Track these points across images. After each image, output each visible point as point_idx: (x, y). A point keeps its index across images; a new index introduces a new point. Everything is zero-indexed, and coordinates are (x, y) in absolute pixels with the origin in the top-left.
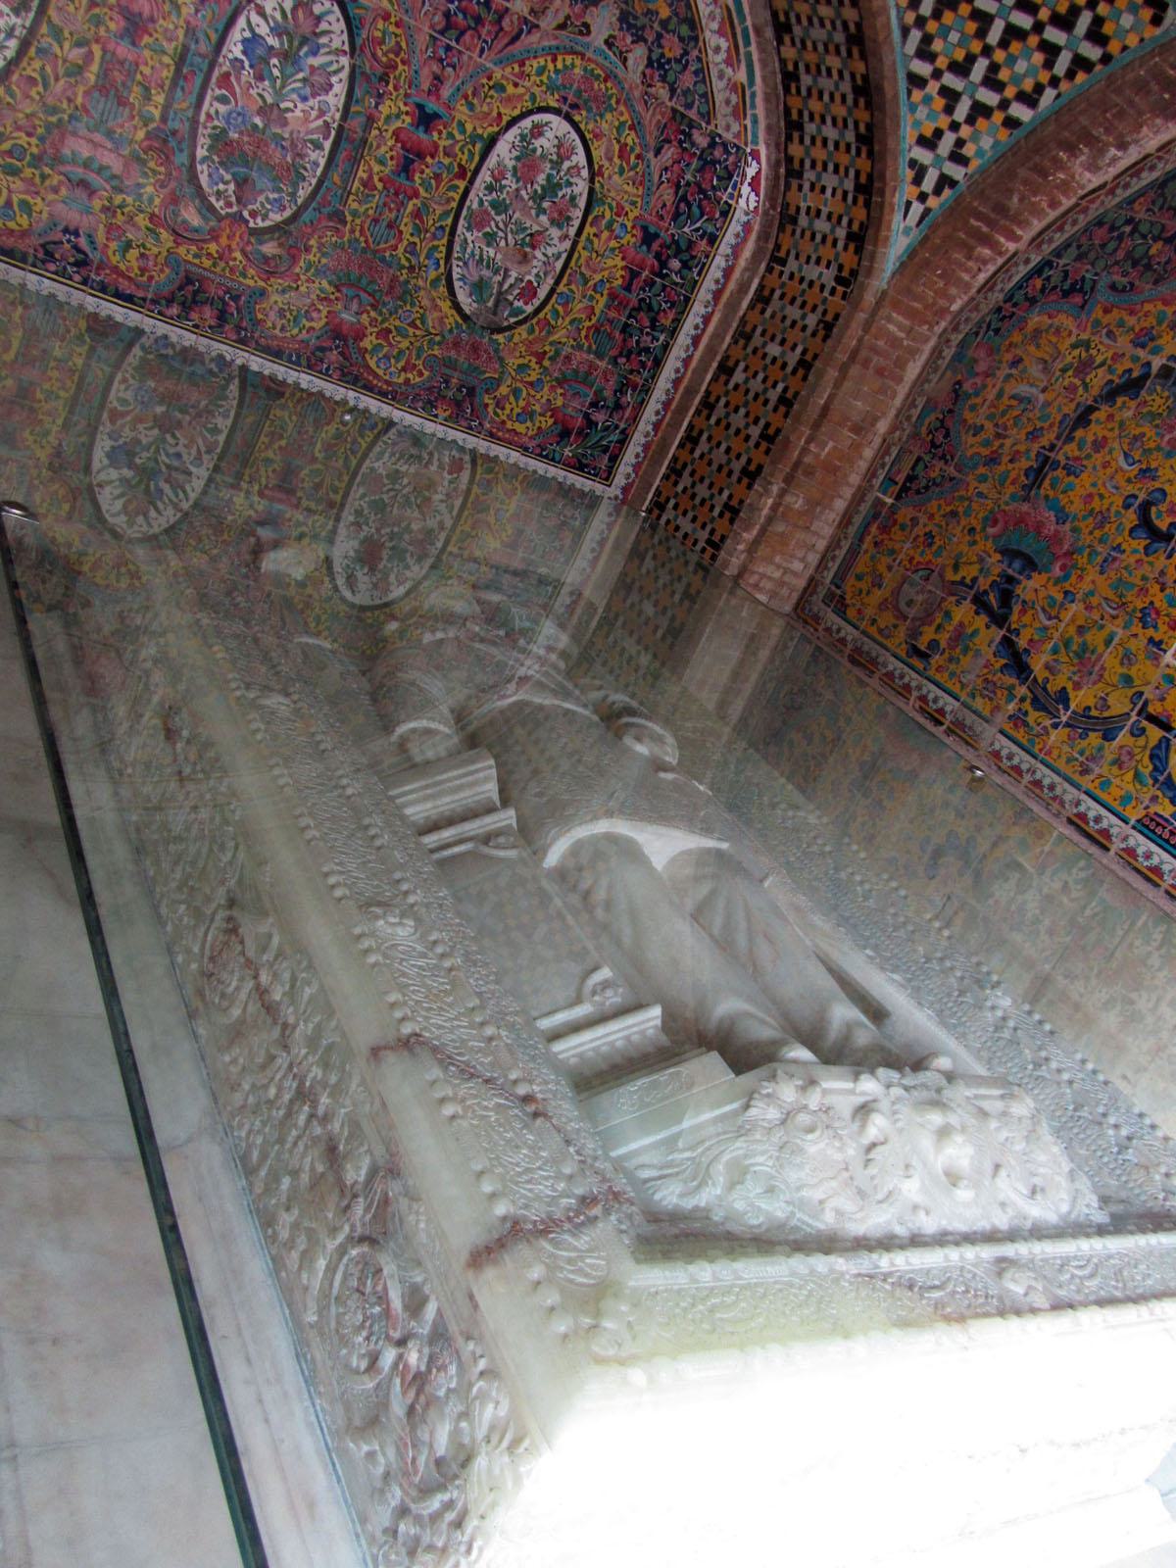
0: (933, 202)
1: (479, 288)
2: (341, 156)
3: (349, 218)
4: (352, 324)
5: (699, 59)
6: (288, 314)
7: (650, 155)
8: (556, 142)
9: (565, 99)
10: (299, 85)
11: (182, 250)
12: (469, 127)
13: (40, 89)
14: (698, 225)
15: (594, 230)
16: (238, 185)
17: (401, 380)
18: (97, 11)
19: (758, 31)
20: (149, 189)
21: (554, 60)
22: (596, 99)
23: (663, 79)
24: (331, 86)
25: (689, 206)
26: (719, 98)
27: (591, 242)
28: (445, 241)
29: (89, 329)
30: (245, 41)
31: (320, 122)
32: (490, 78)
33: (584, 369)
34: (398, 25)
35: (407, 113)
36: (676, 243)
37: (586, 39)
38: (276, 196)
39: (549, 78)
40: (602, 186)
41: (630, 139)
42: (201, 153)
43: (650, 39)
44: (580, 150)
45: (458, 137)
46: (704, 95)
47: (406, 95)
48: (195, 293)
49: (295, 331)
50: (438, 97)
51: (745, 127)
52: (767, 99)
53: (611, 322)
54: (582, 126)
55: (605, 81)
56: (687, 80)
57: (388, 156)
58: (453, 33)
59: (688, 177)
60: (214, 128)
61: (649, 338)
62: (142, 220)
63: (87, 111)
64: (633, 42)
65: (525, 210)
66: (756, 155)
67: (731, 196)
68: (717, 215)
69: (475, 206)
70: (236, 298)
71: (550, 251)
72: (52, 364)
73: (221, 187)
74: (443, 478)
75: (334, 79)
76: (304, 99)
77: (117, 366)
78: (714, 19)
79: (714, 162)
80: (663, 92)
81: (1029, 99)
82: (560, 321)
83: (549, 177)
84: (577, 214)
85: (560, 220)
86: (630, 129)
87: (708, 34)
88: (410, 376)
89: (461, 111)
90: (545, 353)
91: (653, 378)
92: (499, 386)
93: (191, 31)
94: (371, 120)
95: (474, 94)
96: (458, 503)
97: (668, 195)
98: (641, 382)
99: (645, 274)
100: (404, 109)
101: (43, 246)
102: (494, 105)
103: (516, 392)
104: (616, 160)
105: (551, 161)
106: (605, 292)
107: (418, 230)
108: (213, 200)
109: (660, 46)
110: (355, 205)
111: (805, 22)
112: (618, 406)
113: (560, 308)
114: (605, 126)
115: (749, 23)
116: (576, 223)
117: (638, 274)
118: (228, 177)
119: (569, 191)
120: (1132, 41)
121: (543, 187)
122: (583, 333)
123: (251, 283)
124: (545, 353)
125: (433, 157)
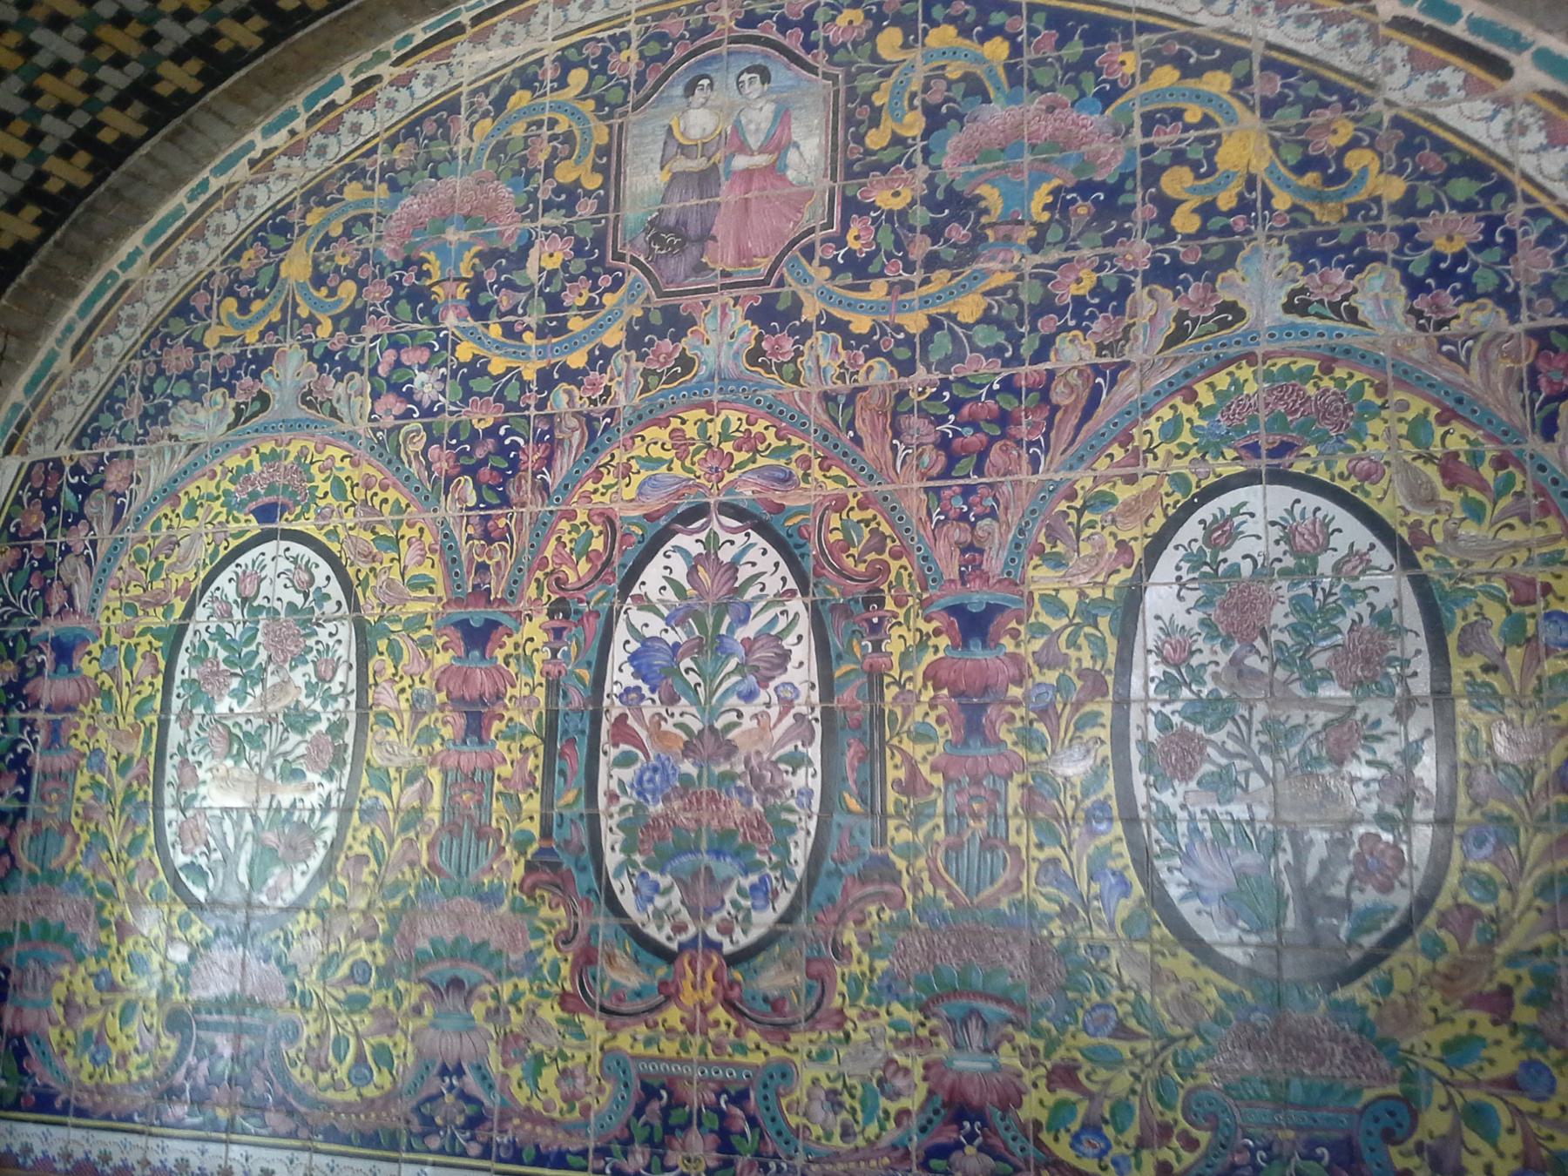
2: (850, 756)
3: (901, 864)
4: (984, 1074)
5: (1537, 213)
6: (846, 1098)
7: (1534, 443)
8: (1276, 532)
9: (1254, 449)
10: (735, 679)
11: (623, 1041)
12: (1070, 598)
13: (373, 865)
16: (686, 888)
18: (425, 721)
20: (550, 953)
21: (1191, 397)
22: (1325, 413)
23: (1469, 293)
24: (786, 656)
28: (1118, 829)
30: (633, 658)
31: (789, 720)
32: (1072, 496)
34: (862, 506)
35: (937, 632)
37: (1241, 327)
38: (754, 878)
39: (1194, 431)
40: (1442, 562)
42: (612, 859)
43: (1389, 249)
45: (1055, 624)
47: (924, 604)
48: (666, 1112)
54: (1322, 475)
55: (1327, 370)
57: (931, 720)
58: (967, 464)
60: (624, 809)
62: (550, 1013)
64: (1350, 275)
69: (1154, 734)
70: (740, 1098)
73: (660, 902)
75: (791, 639)
76: (749, 696)
78: (1524, 130)
80: (1482, 317)
83: (1298, 604)
86: (1443, 420)
87: (1527, 163)
89: (1041, 578)
92: (1414, 1116)
93: (554, 687)
94: (875, 678)
95: (1052, 538)
100: (928, 628)
101: (417, 1110)
102: (1101, 537)
103: (1478, 1117)
104: (1445, 495)
105: (1285, 573)
107: (1048, 834)
108: (651, 930)
110: (905, 835)
118: (665, 881)
121: (1294, 629)
123: (757, 1059)
124: (1506, 991)
125: (1019, 682)
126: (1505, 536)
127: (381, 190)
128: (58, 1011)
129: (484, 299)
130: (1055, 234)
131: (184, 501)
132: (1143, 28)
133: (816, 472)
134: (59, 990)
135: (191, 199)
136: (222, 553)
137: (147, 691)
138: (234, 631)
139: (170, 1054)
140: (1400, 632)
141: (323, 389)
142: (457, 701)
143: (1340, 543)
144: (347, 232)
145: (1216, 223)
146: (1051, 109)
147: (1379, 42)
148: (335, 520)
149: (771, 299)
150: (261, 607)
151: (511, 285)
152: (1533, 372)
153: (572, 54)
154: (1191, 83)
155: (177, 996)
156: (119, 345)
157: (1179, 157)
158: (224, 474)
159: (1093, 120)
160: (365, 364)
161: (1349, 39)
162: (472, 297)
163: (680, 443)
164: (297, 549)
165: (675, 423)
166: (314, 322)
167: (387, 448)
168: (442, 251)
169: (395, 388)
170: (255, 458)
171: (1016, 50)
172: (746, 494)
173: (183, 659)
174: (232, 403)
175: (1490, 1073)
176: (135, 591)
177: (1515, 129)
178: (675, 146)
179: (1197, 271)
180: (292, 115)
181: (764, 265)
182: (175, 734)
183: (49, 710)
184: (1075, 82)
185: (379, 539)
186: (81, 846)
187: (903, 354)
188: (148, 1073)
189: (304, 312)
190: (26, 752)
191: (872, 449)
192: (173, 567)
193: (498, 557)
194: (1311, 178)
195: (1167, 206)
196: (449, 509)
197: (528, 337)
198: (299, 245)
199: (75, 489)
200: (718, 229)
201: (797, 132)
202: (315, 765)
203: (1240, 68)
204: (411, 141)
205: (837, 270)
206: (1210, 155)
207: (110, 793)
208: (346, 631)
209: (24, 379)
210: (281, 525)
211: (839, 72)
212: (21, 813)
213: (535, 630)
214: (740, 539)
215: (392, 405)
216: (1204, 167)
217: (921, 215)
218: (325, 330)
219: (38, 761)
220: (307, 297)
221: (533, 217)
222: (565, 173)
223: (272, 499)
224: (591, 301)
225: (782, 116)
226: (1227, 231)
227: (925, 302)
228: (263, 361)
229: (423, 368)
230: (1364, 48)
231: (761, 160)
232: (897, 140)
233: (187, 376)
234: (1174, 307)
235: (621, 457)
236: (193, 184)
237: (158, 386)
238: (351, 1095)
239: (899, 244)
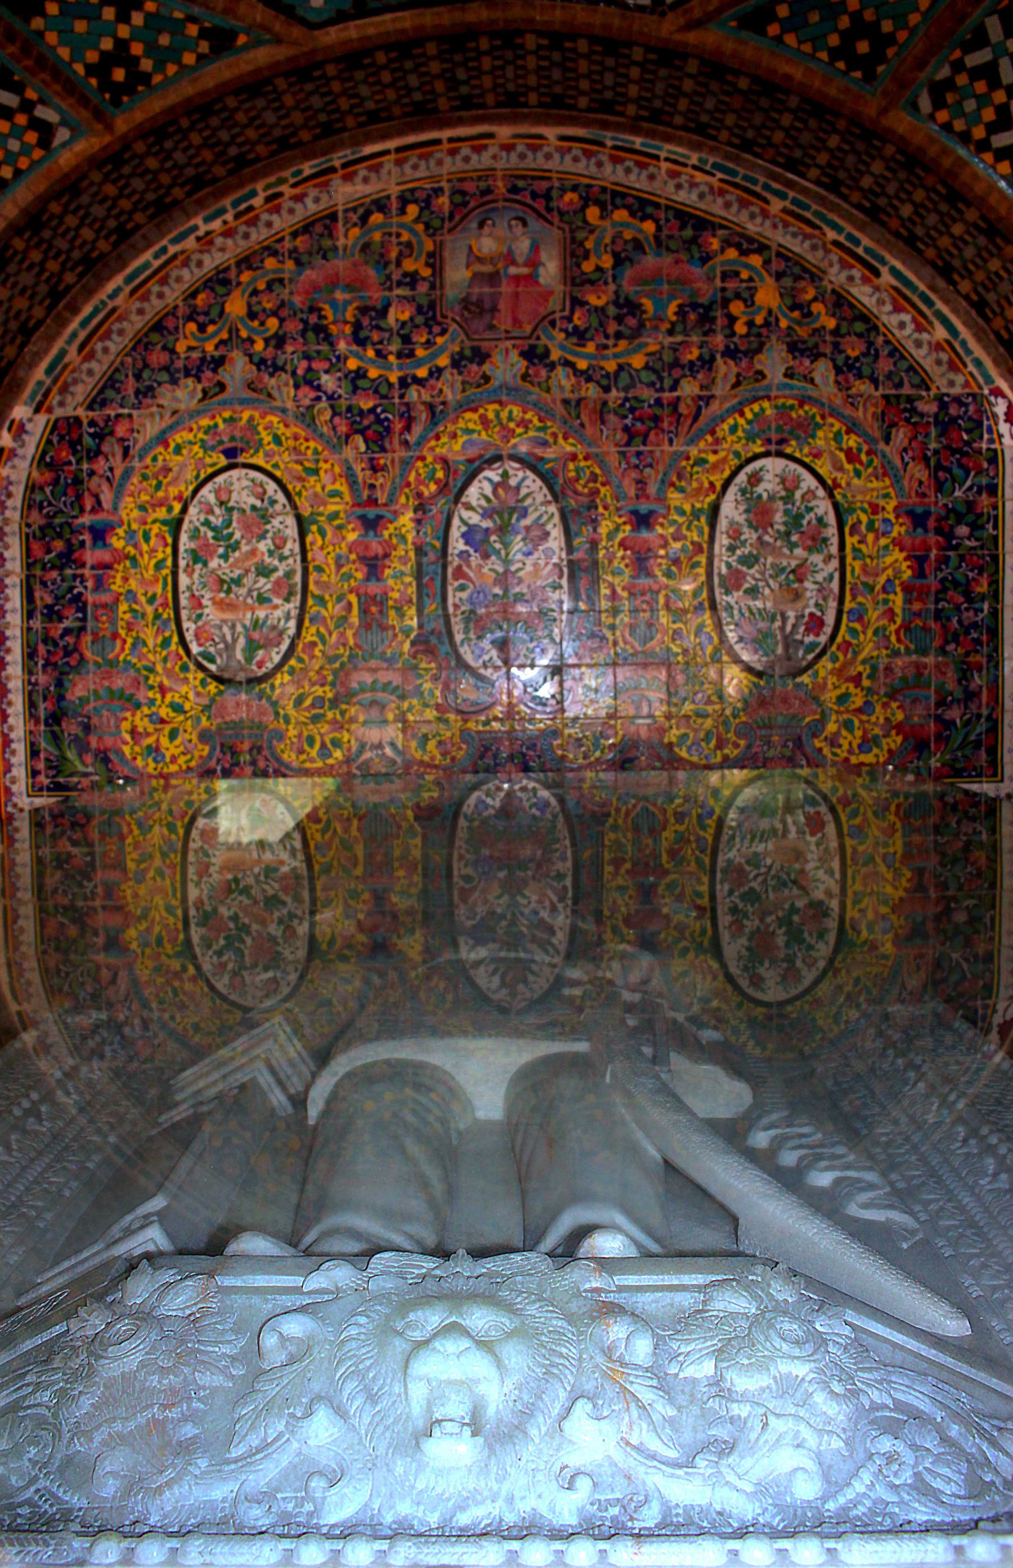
1: (759, 641)
5: (887, 342)
7: (881, 446)
9: (769, 441)
11: (471, 725)
12: (687, 508)
13: (320, 647)
14: (969, 483)
15: (856, 539)
17: (719, 759)
18: (344, 570)
19: (932, 288)
20: (427, 686)
21: (742, 414)
23: (860, 376)
24: (547, 534)
25: (949, 470)
26: (928, 364)
27: (860, 550)
29: (417, 818)
30: (464, 535)
31: (550, 567)
32: (688, 458)
33: (911, 672)
34: (586, 459)
36: (953, 510)
37: (765, 382)
40: (844, 496)
41: (852, 441)
42: (459, 637)
46: (911, 368)
47: (618, 509)
49: (598, 754)
50: (647, 497)
51: (971, 374)
52: (979, 339)
53: (918, 614)
54: (798, 455)
56: (884, 365)
58: (638, 440)
59: (933, 445)
61: (971, 613)
63: (360, 647)
65: (775, 551)
66: (997, 392)
67: (991, 441)
68: (985, 465)
69: (724, 570)
71: (819, 578)
72: (396, 865)
74: (808, 843)
76: (529, 554)
77: (451, 844)
78: (884, 303)
79: (954, 420)
80: (863, 387)
82: (862, 637)
83: (786, 512)
84: (831, 532)
85: (816, 542)
86: (848, 432)
87: (885, 318)
88: (726, 751)
89: (674, 497)
90: (860, 674)
91: (996, 650)
93: (420, 551)
94: (594, 544)
95: (680, 477)
96: (836, 865)
97: (919, 472)
98: (984, 661)
99: (933, 553)
100: (620, 521)
106: (898, 589)
109: (841, 352)
111: (955, 252)
112: (971, 696)
113: (857, 626)
114: (820, 443)
115: (922, 287)
116: (835, 541)
117: (926, 558)
119: (812, 515)
121: (785, 524)
122: (893, 638)
124: (860, 674)
126: (870, 485)
127: (290, 265)
128: (128, 737)
129: (363, 334)
130: (679, 328)
131: (172, 445)
132: (722, 227)
133: (561, 441)
134: (126, 726)
135: (156, 256)
136: (203, 476)
137: (160, 556)
138: (216, 521)
139: (205, 753)
140: (826, 526)
141: (261, 381)
142: (362, 559)
143: (804, 486)
144: (269, 287)
145: (755, 331)
146: (677, 262)
147: (827, 251)
148: (277, 458)
149: (533, 347)
150: (232, 509)
151: (378, 328)
152: (883, 414)
153: (408, 195)
154: (743, 259)
155: (204, 722)
156: (113, 348)
157: (738, 296)
158: (199, 429)
159: (698, 271)
160: (288, 367)
161: (814, 248)
162: (355, 333)
163: (485, 421)
165: (481, 411)
166: (251, 341)
167: (307, 417)
168: (333, 304)
169: (309, 383)
170: (219, 420)
171: (659, 229)
172: (523, 449)
173: (184, 538)
174: (200, 387)
175: (853, 707)
176: (145, 498)
177: (881, 302)
178: (473, 258)
179: (745, 353)
180: (223, 211)
181: (528, 329)
182: (184, 580)
183: (93, 568)
184: (689, 250)
185: (306, 470)
186: (128, 646)
187: (605, 382)
188: (193, 764)
189: (244, 334)
190: (80, 594)
191: (589, 430)
192: (169, 484)
193: (381, 480)
194: (796, 314)
195: (732, 320)
196: (349, 453)
197: (392, 358)
198: (237, 293)
199: (93, 436)
200: (502, 305)
201: (544, 256)
202: (277, 594)
203: (766, 254)
204: (306, 237)
205: (568, 335)
206: (752, 296)
207: (144, 615)
208: (291, 521)
209: (44, 365)
210: (241, 460)
211: (567, 228)
212: (82, 629)
213: (406, 520)
214: (521, 474)
215: (307, 395)
216: (749, 302)
217: (612, 310)
218: (259, 346)
219: (90, 598)
220: (245, 325)
221: (390, 289)
222: (409, 265)
223: (233, 444)
224: (428, 342)
225: (535, 248)
226: (759, 335)
227: (615, 356)
228: (219, 363)
229: (327, 372)
230: (820, 253)
231: (525, 271)
232: (599, 269)
233: (166, 369)
235: (451, 428)
236: (156, 248)
237: (146, 374)
238: (319, 764)
239: (601, 324)
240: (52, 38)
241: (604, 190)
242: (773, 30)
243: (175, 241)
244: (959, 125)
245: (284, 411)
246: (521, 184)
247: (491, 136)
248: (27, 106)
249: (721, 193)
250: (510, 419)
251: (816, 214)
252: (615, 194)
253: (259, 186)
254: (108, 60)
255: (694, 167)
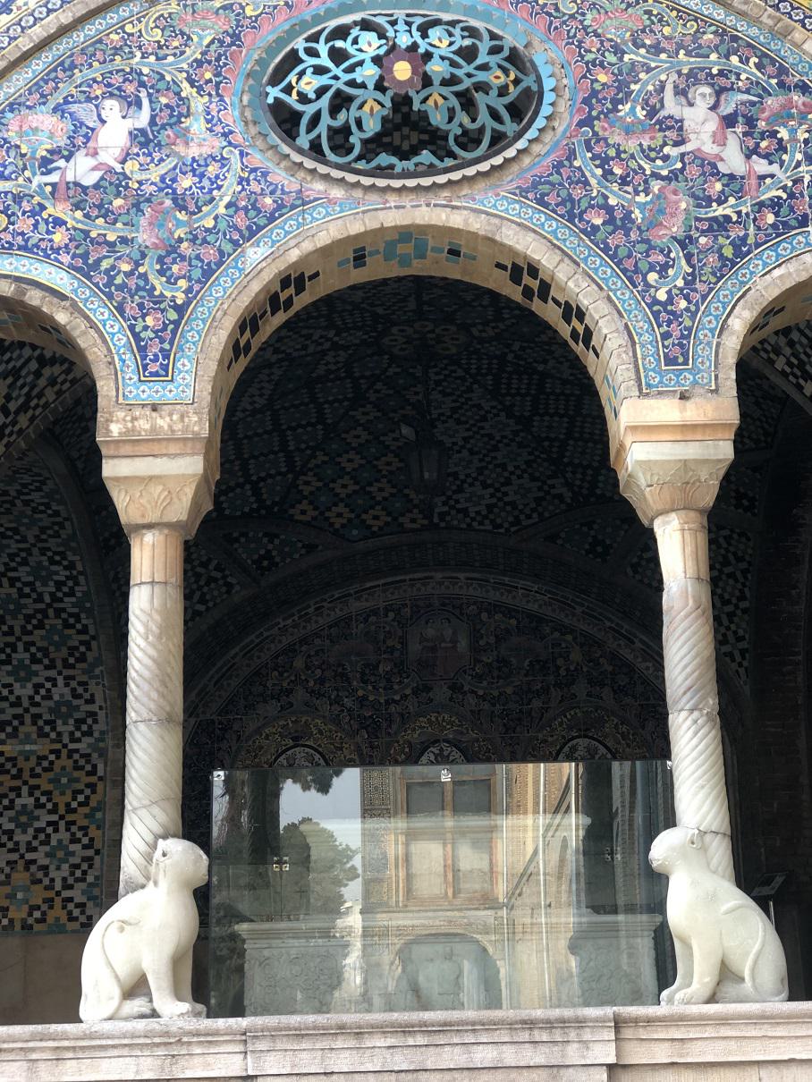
0: (745, 663)
9: (580, 730)
21: (566, 717)
41: (624, 728)
44: (601, 747)
80: (628, 700)
81: (742, 598)
120: (750, 551)
127: (327, 642)
132: (552, 621)
135: (257, 637)
143: (600, 752)
144: (317, 653)
151: (373, 674)
163: (430, 721)
164: (307, 750)
167: (336, 721)
171: (519, 622)
180: (294, 615)
189: (303, 678)
195: (558, 668)
196: (358, 739)
209: (196, 691)
215: (336, 708)
217: (495, 664)
218: (311, 683)
222: (390, 643)
228: (289, 692)
231: (450, 645)
234: (561, 694)
236: (258, 633)
240: (240, 551)
241: (490, 604)
242: (560, 542)
243: (268, 630)
244: (646, 581)
245: (324, 717)
246: (447, 601)
247: (431, 578)
248: (224, 577)
249: (551, 605)
250: (443, 720)
251: (601, 614)
252: (495, 606)
253: (312, 602)
254: (262, 558)
255: (536, 592)
